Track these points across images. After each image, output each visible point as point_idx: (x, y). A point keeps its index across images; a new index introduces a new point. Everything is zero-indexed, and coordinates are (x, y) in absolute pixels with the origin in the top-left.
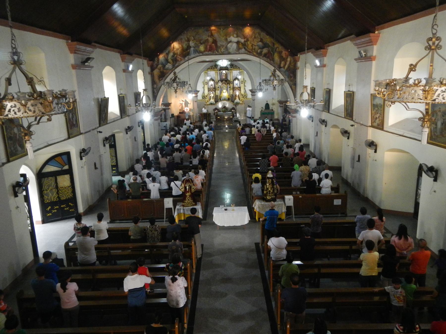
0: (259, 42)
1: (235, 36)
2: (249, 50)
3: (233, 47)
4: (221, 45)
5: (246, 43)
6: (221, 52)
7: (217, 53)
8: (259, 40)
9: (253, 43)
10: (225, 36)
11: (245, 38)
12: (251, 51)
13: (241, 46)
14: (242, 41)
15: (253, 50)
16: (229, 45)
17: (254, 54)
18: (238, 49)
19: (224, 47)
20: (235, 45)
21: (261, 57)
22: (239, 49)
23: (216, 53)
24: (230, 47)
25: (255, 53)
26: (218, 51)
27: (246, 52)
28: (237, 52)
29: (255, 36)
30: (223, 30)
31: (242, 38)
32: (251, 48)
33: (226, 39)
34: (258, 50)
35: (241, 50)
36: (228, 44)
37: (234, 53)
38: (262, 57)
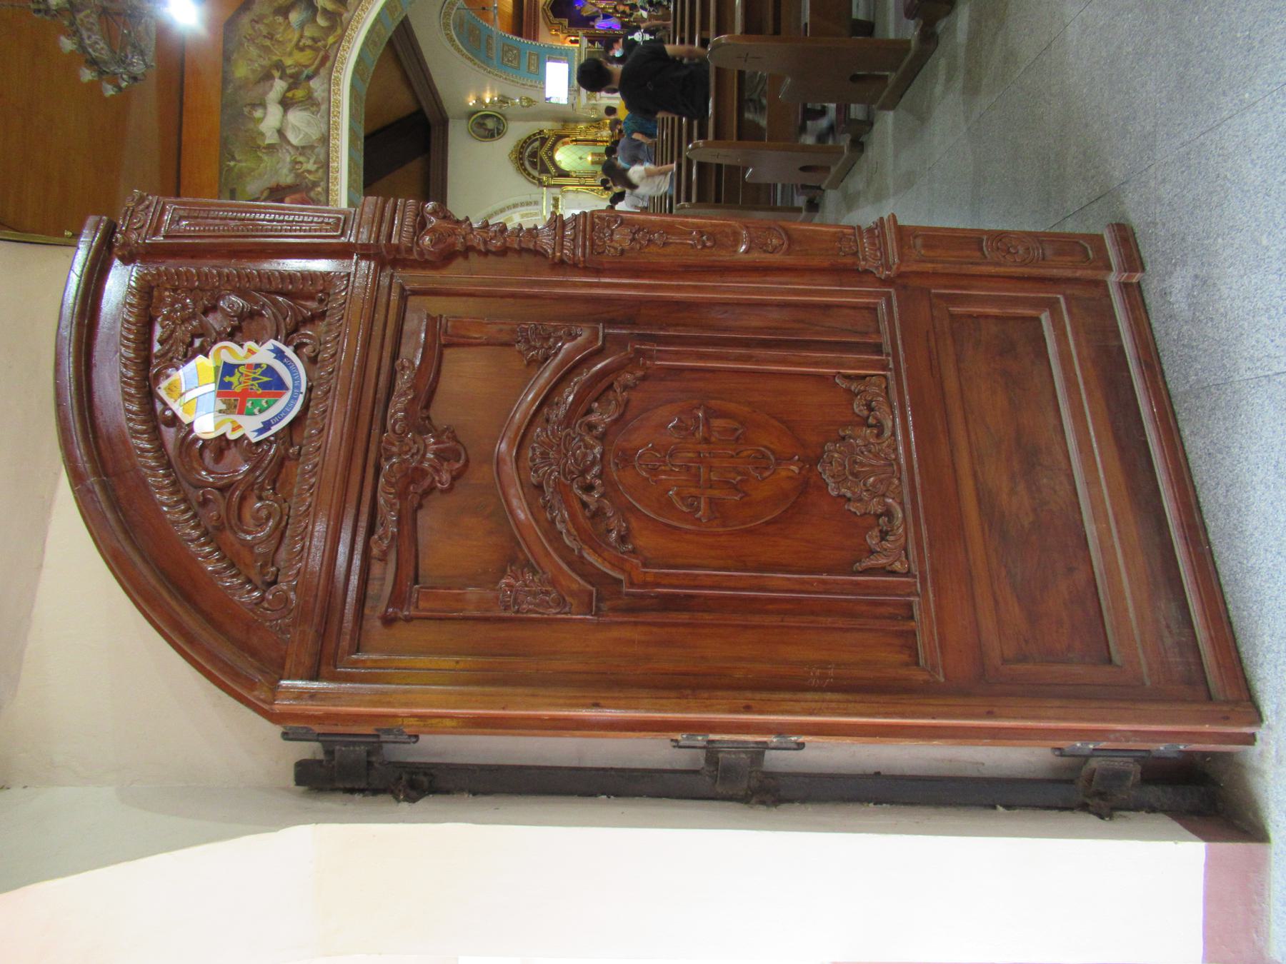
0: (289, 23)
1: (258, 114)
2: (317, 62)
3: (300, 125)
4: (291, 171)
5: (288, 71)
6: (318, 168)
7: (319, 189)
8: (280, 19)
9: (289, 47)
10: (260, 155)
11: (267, 77)
12: (322, 53)
13: (300, 93)
14: (279, 86)
15: (320, 44)
16: (294, 139)
17: (335, 43)
18: (312, 106)
19: (301, 159)
20: (296, 117)
21: (346, 16)
22: (310, 102)
23: (319, 193)
24: (301, 136)
25: (331, 40)
26: (315, 184)
27: (323, 72)
28: (324, 107)
29: (265, 37)
30: (233, 158)
31: (272, 86)
32: (308, 53)
33: (271, 148)
34: (319, 26)
35: (316, 95)
36: (289, 143)
37: (326, 119)
38: (347, 11)
